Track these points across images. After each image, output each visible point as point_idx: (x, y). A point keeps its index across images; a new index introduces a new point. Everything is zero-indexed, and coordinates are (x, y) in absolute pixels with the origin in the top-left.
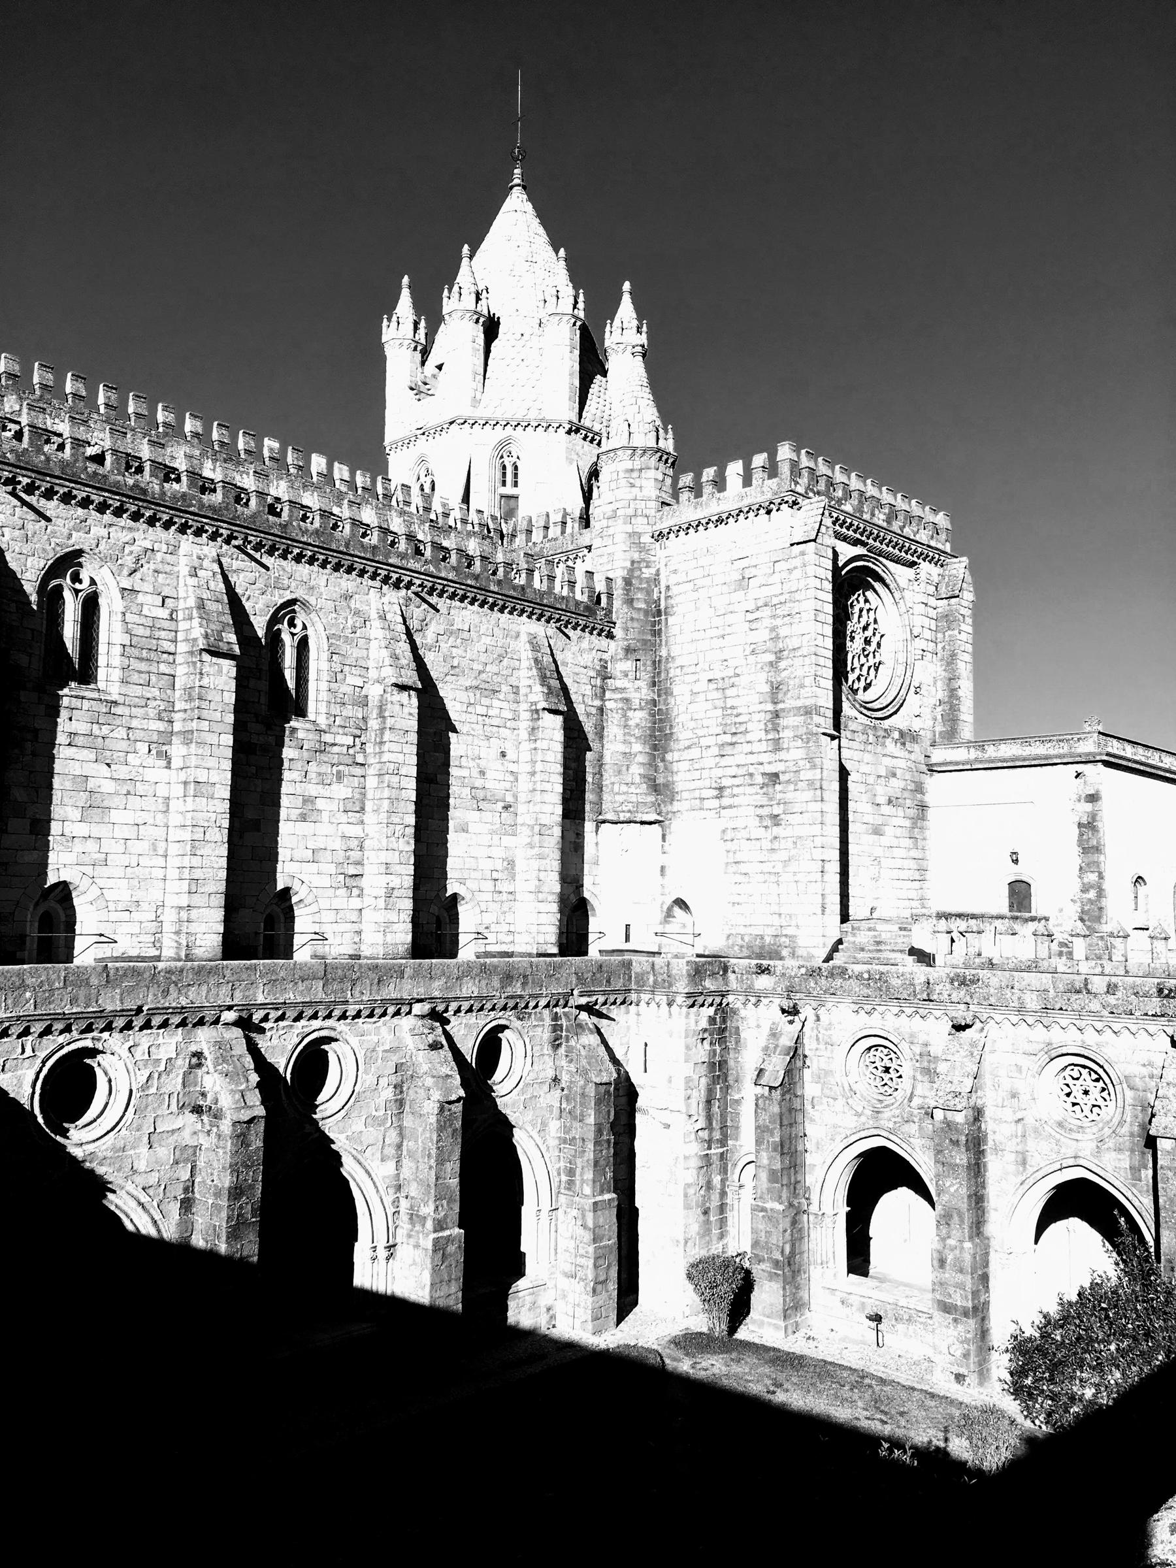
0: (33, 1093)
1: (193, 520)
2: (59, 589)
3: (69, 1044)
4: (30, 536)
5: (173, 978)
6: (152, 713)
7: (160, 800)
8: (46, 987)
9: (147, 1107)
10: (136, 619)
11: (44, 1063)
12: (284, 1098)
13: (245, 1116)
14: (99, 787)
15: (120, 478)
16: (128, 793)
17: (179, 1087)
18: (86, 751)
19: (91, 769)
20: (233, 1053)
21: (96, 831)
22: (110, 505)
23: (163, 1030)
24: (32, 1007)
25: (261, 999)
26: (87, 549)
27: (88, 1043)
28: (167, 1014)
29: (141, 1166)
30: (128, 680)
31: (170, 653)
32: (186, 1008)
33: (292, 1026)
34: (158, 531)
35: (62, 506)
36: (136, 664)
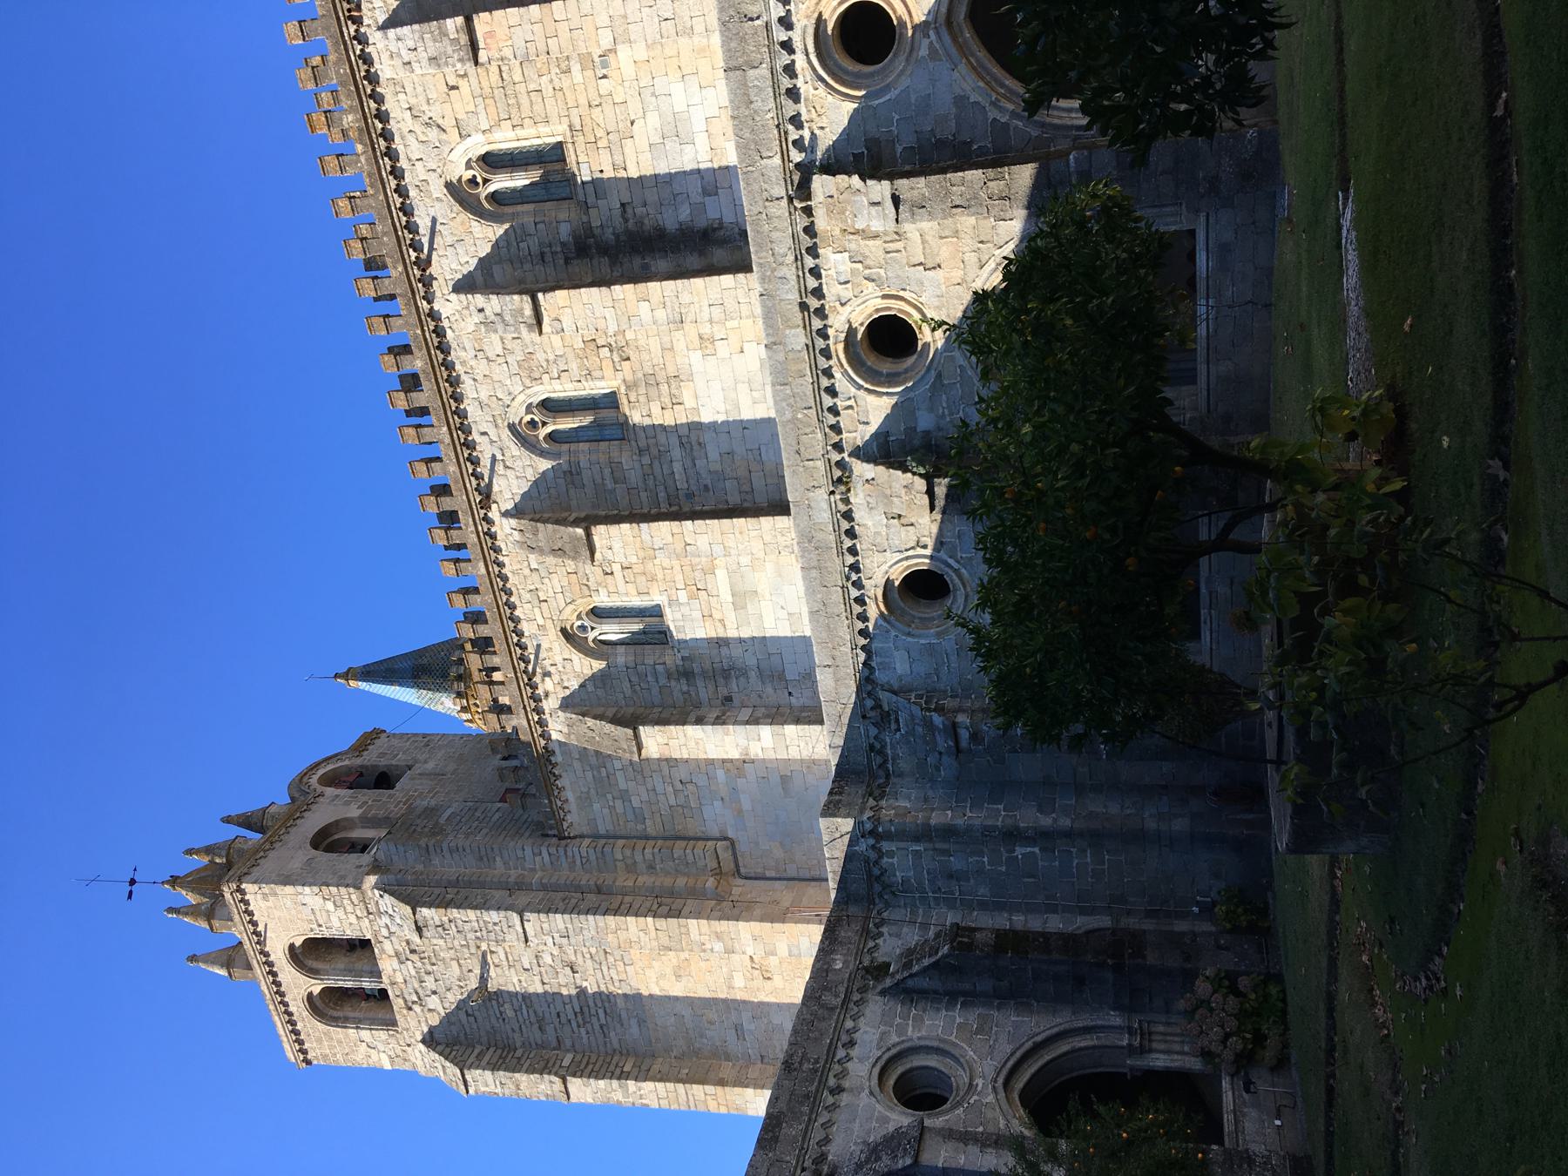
0: (887, 394)
1: (359, 71)
2: (494, 197)
3: (842, 365)
4: (456, 239)
5: (769, 273)
6: (566, 82)
7: (652, 54)
8: (792, 401)
9: (898, 277)
10: (482, 116)
11: (860, 387)
12: (887, 97)
13: (889, 203)
14: (656, 129)
15: (363, 159)
16: (653, 94)
17: (878, 242)
18: (627, 151)
19: (641, 141)
20: (836, 196)
21: (699, 125)
22: (391, 167)
23: (822, 271)
24: (810, 411)
25: (777, 160)
26: (442, 181)
27: (841, 347)
28: (804, 273)
29: (957, 275)
30: (544, 116)
31: (500, 70)
32: (796, 256)
33: (806, 100)
34: (389, 105)
35: (416, 213)
36: (526, 112)
